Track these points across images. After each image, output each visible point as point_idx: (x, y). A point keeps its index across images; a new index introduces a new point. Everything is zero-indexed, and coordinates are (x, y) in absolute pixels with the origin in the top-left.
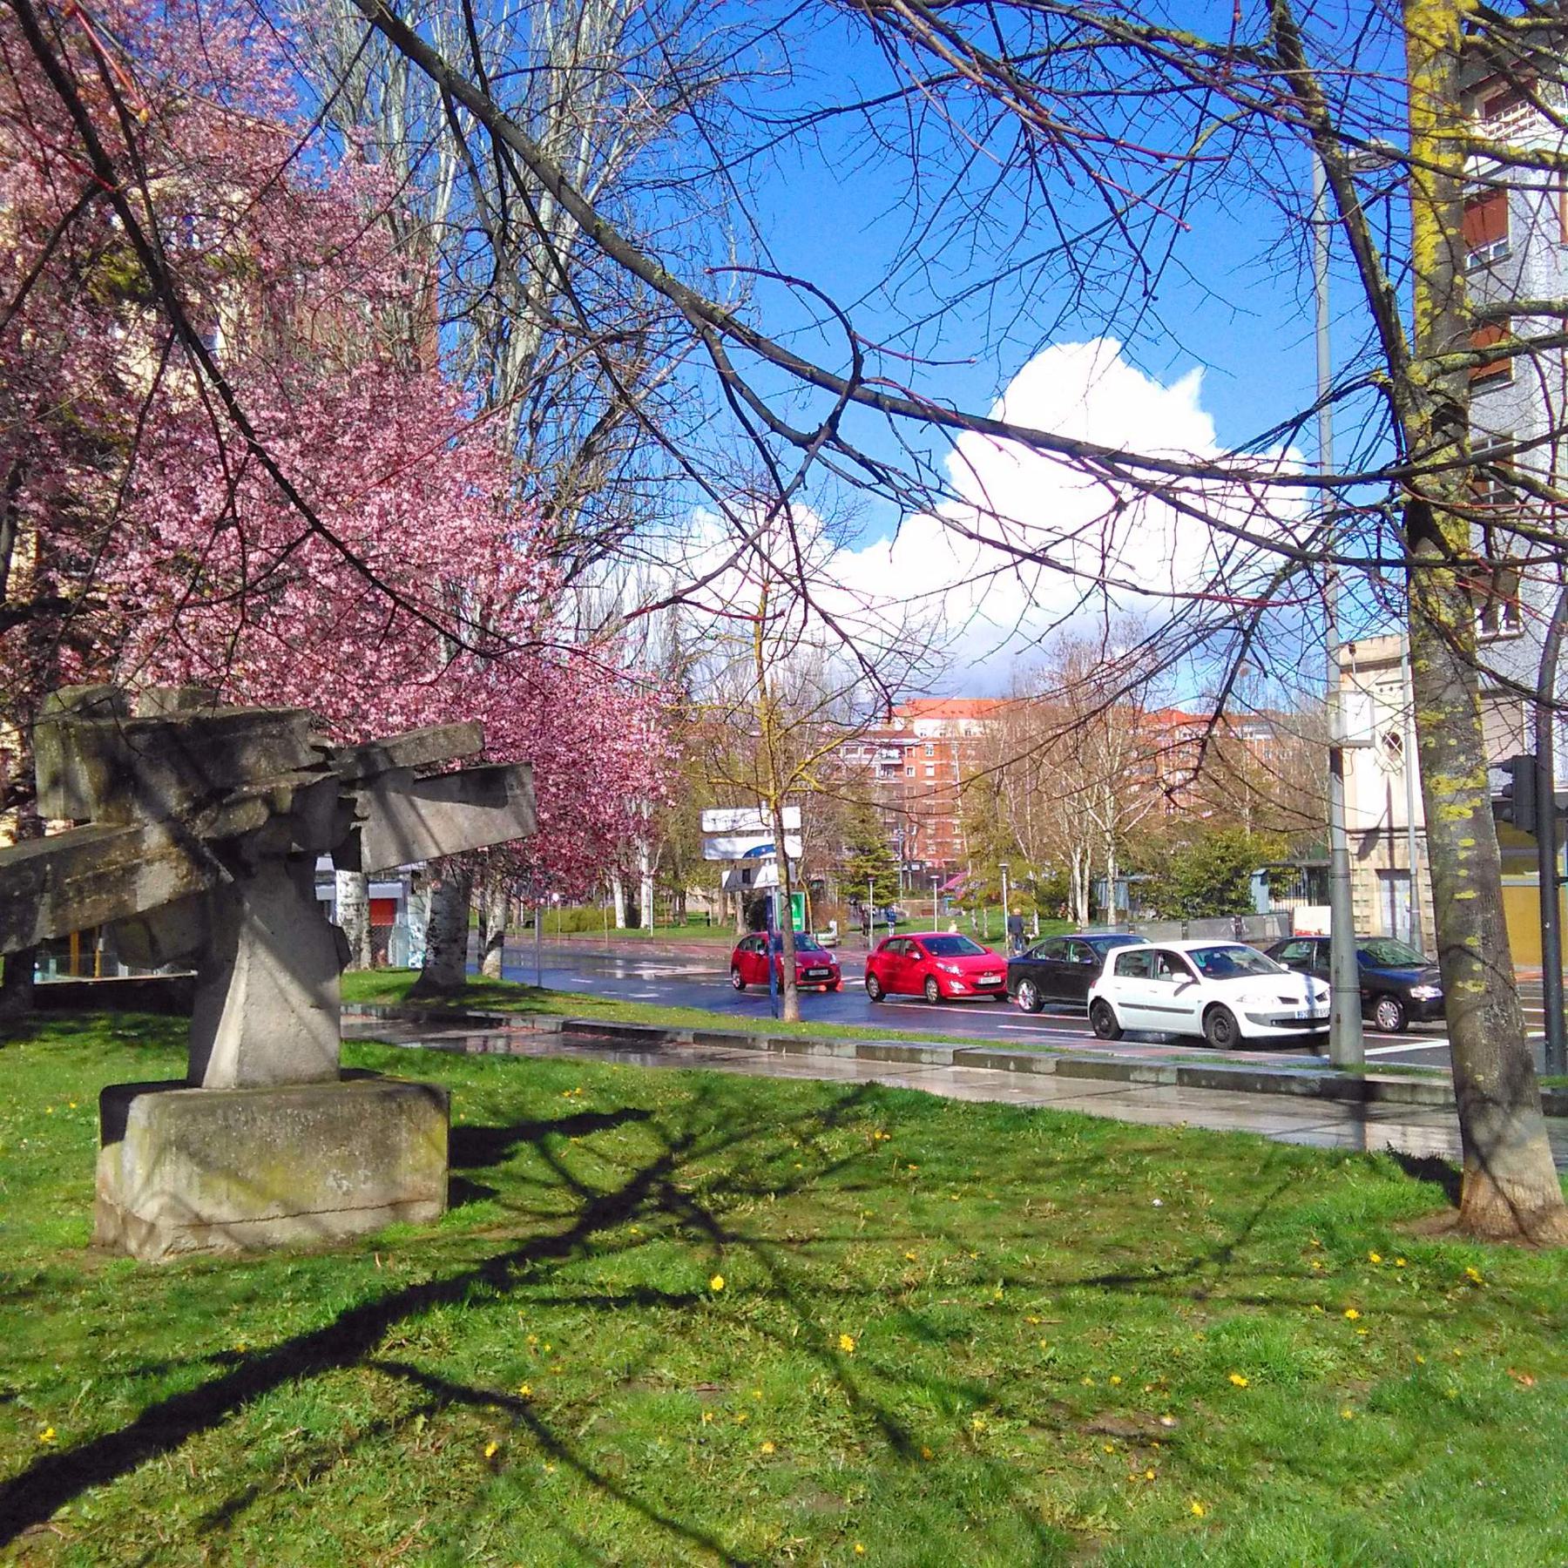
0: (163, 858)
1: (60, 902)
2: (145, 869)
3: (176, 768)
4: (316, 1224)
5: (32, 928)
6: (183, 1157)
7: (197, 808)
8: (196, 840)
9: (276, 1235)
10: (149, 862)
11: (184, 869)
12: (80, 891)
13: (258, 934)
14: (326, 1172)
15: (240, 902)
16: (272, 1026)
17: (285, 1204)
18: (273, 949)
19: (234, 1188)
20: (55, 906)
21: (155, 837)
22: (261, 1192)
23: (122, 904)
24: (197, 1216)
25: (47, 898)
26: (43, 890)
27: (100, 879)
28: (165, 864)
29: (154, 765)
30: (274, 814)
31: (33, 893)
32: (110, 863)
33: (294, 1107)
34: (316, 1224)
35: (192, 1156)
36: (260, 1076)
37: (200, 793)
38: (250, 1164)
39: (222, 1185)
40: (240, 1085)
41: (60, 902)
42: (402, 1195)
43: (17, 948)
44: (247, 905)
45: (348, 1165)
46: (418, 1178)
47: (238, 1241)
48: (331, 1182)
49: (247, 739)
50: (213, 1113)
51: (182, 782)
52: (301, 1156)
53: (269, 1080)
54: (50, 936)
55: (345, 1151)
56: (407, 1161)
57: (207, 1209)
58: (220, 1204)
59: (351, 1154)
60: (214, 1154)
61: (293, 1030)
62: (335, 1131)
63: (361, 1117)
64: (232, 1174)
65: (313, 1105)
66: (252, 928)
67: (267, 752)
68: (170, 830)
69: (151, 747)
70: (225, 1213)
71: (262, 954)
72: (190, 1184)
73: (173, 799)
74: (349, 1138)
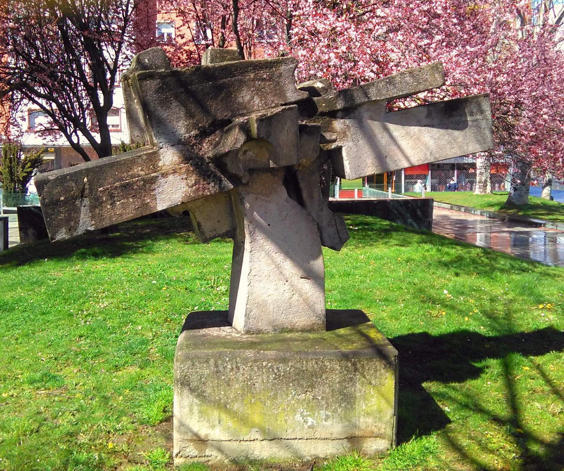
0: (175, 172)
1: (96, 204)
2: (162, 180)
3: (183, 104)
4: (288, 447)
5: (77, 222)
6: (186, 391)
7: (204, 134)
8: (202, 159)
9: (257, 453)
10: (165, 175)
11: (193, 179)
12: (112, 196)
13: (257, 226)
14: (295, 411)
15: (243, 204)
16: (271, 292)
17: (262, 431)
18: (270, 236)
19: (223, 416)
20: (93, 208)
21: (169, 157)
22: (244, 420)
23: (145, 205)
24: (196, 435)
25: (86, 201)
26: (82, 196)
27: (126, 187)
28: (177, 177)
29: (165, 103)
30: (249, 138)
31: (75, 198)
32: (133, 176)
33: (269, 361)
34: (288, 447)
35: (192, 391)
36: (263, 325)
37: (205, 123)
38: (235, 399)
39: (215, 414)
40: (248, 332)
41: (96, 204)
42: (358, 433)
43: (67, 237)
44: (247, 205)
45: (313, 406)
46: (370, 420)
47: (227, 456)
48: (298, 417)
49: (242, 83)
50: (207, 362)
51: (190, 115)
52: (275, 397)
53: (270, 329)
54: (92, 229)
55: (310, 396)
56: (361, 406)
57: (203, 430)
58: (213, 426)
59: (314, 398)
60: (209, 391)
61: (287, 295)
62: (307, 380)
63: (323, 370)
64: (223, 406)
65: (284, 360)
66: (252, 221)
67: (259, 91)
68: (181, 151)
69: (160, 90)
70: (216, 434)
71: (261, 238)
72: (191, 410)
73: (182, 128)
74: (312, 386)
